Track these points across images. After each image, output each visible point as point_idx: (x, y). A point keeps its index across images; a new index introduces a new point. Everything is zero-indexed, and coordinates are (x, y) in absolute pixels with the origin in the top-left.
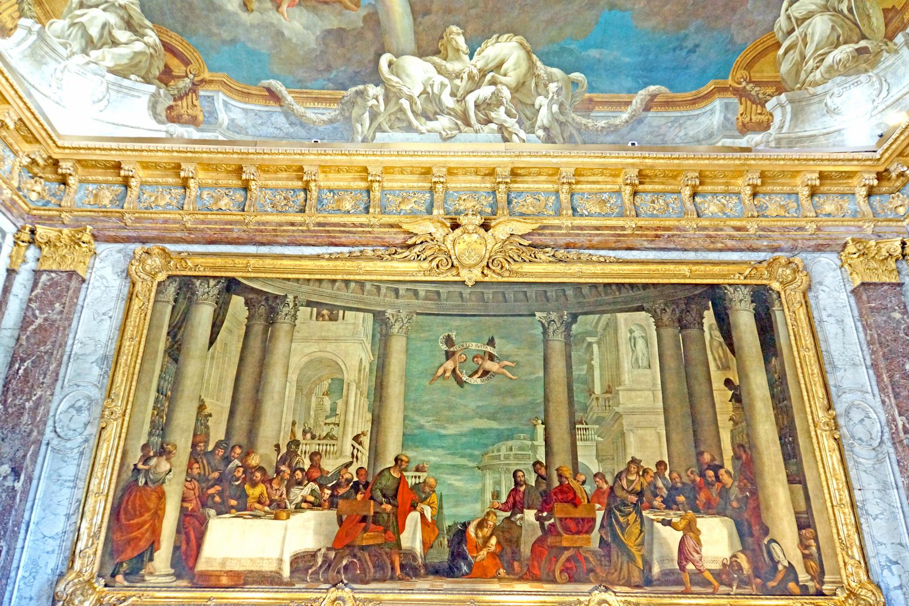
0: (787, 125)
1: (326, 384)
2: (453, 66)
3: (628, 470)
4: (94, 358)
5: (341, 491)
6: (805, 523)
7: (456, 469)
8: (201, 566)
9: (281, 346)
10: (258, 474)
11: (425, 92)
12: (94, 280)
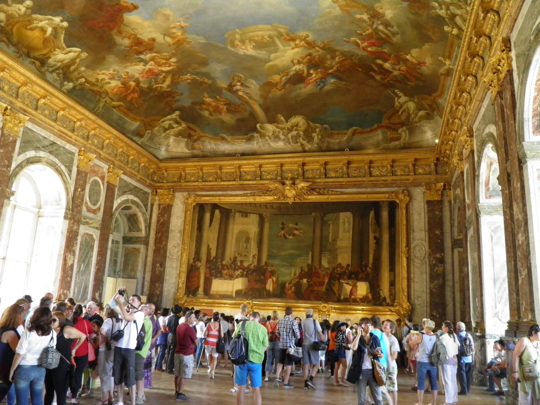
0: (407, 138)
1: (244, 239)
2: (280, 126)
3: (337, 267)
4: (177, 231)
5: (249, 272)
6: (392, 284)
7: (283, 266)
8: (211, 293)
9: (231, 226)
10: (225, 267)
11: (273, 134)
12: (175, 205)
